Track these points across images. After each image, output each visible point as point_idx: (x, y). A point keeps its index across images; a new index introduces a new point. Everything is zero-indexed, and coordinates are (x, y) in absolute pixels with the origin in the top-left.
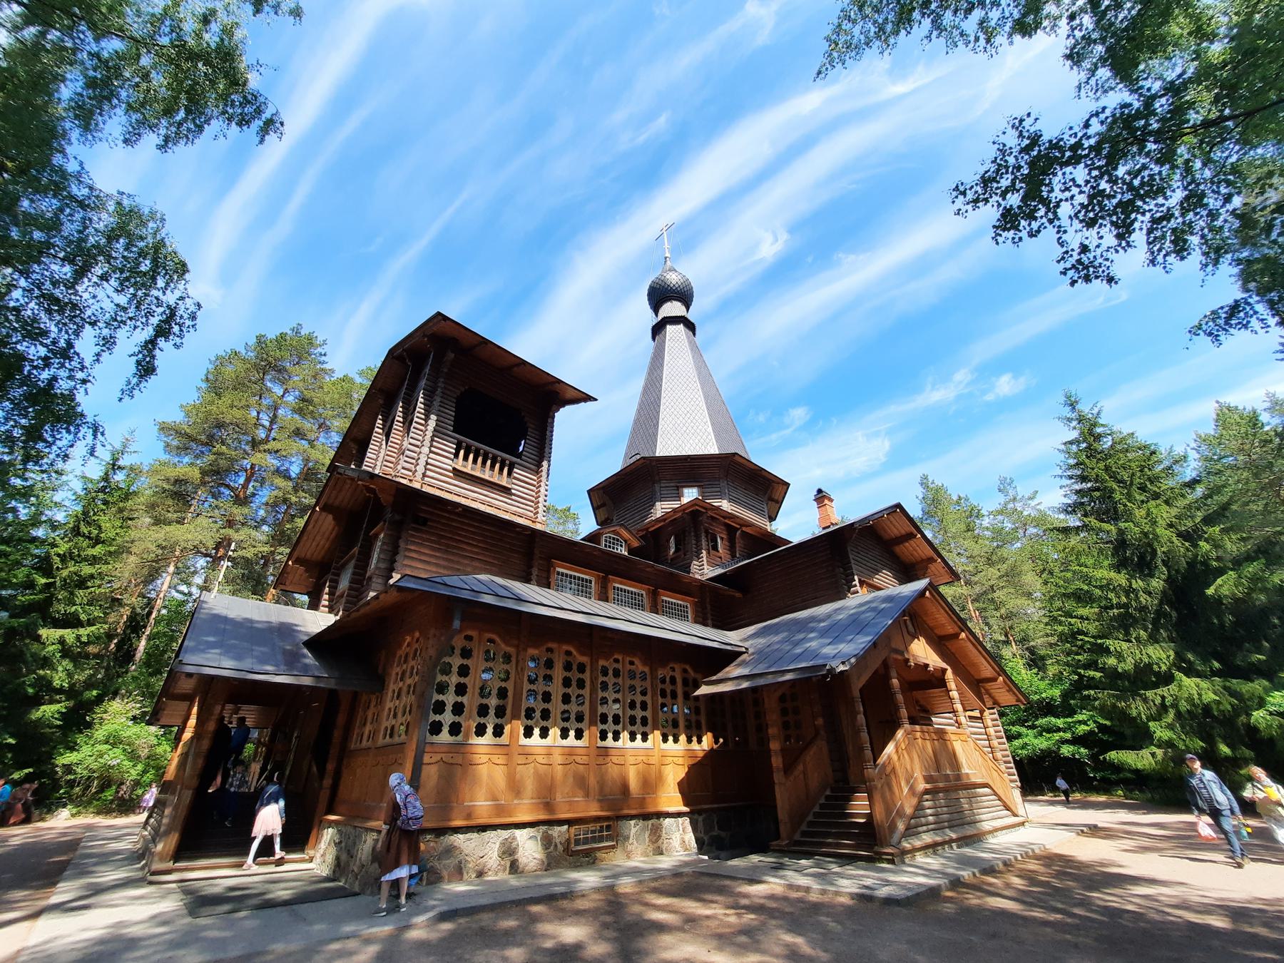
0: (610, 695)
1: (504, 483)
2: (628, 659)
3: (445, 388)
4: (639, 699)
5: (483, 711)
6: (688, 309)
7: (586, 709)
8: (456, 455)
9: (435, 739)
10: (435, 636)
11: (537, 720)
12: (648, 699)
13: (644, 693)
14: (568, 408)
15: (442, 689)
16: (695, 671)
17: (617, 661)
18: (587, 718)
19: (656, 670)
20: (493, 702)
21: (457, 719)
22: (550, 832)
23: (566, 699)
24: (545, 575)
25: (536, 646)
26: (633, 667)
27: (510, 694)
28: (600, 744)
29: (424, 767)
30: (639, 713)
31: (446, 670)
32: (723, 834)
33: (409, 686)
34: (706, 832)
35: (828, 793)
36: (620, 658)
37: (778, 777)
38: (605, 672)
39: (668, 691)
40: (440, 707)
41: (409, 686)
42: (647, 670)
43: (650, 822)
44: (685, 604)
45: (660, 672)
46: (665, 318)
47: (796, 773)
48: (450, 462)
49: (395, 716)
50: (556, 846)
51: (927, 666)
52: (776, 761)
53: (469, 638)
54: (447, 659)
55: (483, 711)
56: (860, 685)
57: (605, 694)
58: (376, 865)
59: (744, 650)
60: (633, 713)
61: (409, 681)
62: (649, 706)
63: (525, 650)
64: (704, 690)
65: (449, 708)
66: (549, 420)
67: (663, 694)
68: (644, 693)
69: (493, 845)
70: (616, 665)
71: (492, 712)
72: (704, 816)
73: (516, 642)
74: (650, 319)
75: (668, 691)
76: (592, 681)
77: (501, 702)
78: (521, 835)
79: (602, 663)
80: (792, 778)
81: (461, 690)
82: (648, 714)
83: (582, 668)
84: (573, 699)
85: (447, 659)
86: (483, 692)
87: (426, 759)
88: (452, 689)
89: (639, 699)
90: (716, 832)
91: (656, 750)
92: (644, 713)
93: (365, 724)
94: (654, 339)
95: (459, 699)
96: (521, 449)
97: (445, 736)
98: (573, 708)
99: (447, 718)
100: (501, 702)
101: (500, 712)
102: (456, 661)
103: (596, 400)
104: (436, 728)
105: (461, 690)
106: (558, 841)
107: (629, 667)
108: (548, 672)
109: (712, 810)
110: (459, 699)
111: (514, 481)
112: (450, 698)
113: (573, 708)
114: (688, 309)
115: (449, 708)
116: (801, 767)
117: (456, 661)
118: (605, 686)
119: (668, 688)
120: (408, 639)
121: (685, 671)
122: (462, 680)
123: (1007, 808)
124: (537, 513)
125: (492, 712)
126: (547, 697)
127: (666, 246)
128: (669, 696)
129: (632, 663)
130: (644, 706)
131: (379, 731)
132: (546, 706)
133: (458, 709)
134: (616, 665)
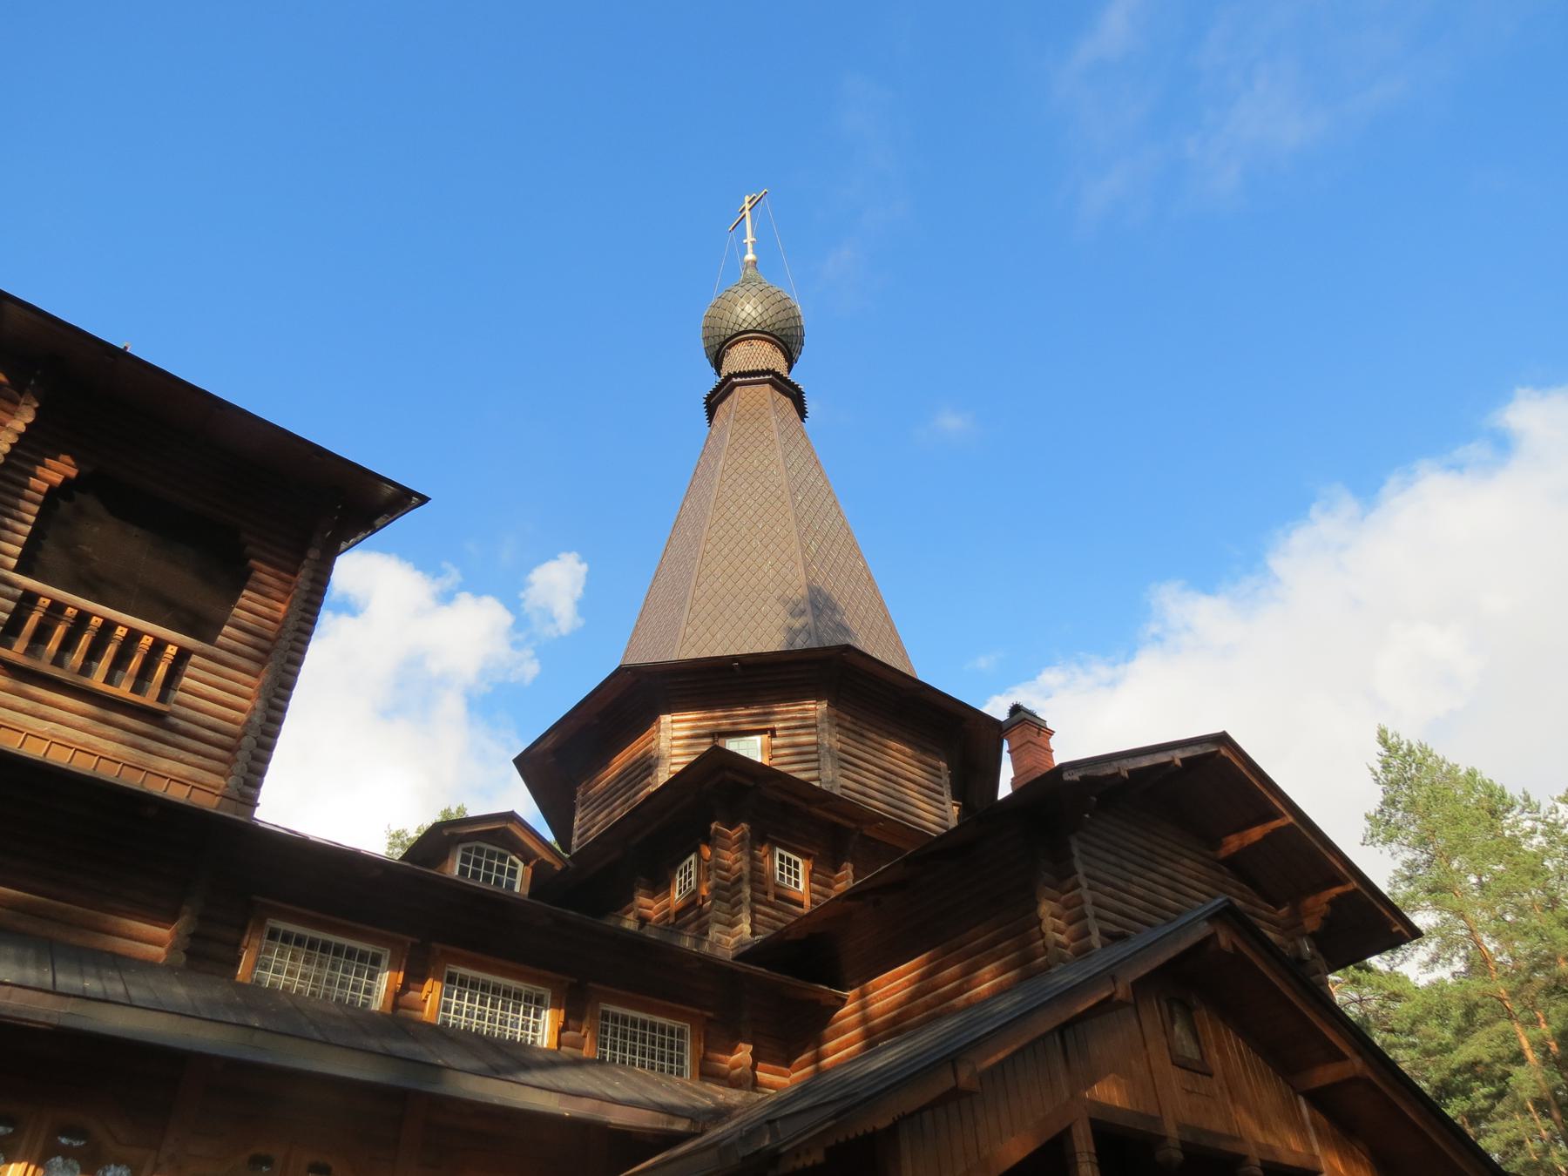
6: (790, 361)
44: (676, 1024)
46: (730, 376)
114: (790, 361)
127: (749, 239)
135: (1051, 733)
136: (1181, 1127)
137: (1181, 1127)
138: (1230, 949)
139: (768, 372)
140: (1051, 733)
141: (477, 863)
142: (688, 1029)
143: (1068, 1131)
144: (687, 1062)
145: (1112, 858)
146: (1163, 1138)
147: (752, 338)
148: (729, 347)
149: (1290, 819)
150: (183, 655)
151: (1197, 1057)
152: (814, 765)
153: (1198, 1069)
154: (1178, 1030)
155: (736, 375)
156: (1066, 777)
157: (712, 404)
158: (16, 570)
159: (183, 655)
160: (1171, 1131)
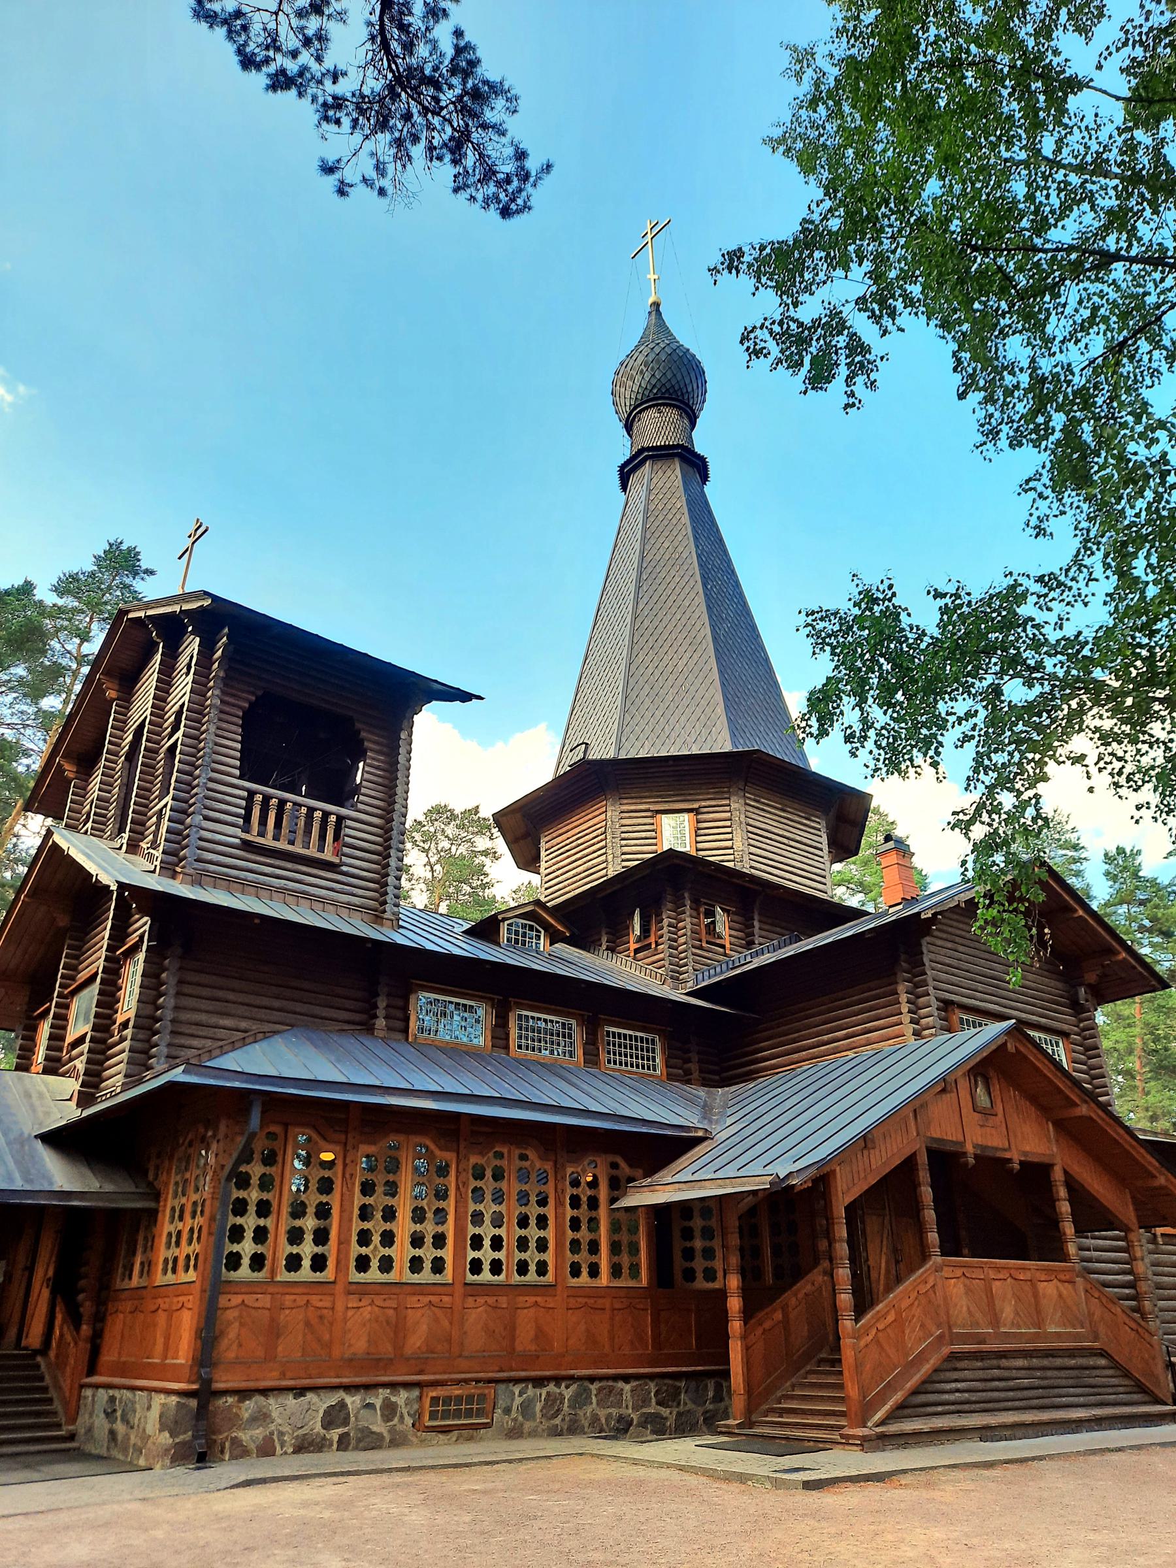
0: (489, 1208)
1: (328, 855)
2: (517, 1152)
3: (222, 712)
4: (534, 1211)
5: (296, 1236)
7: (449, 1228)
8: (247, 818)
9: (234, 1275)
10: (226, 1136)
11: (376, 1247)
12: (549, 1211)
13: (543, 1202)
14: (435, 704)
15: (240, 1208)
16: (631, 1166)
17: (499, 1155)
18: (450, 1241)
19: (564, 1167)
20: (309, 1223)
21: (260, 1249)
22: (393, 1399)
23: (418, 1215)
24: (400, 1003)
25: (374, 1143)
26: (526, 1164)
27: (335, 1212)
28: (471, 1278)
29: (219, 1312)
30: (533, 1233)
31: (243, 1182)
32: (665, 1412)
33: (195, 1204)
34: (635, 1409)
35: (823, 1355)
36: (505, 1151)
37: (736, 1326)
38: (479, 1176)
39: (584, 1199)
40: (237, 1234)
41: (195, 1204)
42: (548, 1166)
43: (544, 1392)
44: (650, 1036)
45: (569, 1170)
47: (767, 1325)
48: (238, 832)
49: (178, 1244)
50: (402, 1417)
51: (1010, 1161)
52: (734, 1304)
53: (272, 1136)
54: (243, 1168)
55: (296, 1236)
56: (848, 1199)
57: (481, 1207)
58: (167, 1434)
59: (700, 1134)
60: (523, 1232)
61: (194, 1197)
62: (551, 1222)
63: (355, 1147)
64: (631, 1200)
65: (249, 1234)
66: (403, 735)
67: (575, 1202)
68: (543, 1202)
69: (314, 1414)
70: (498, 1162)
71: (309, 1237)
72: (634, 1383)
73: (343, 1137)
74: (622, 449)
75: (584, 1199)
76: (458, 1188)
77: (321, 1223)
78: (353, 1402)
79: (474, 1160)
80: (759, 1331)
81: (264, 1209)
82: (550, 1234)
83: (443, 1171)
84: (430, 1215)
85: (243, 1169)
86: (298, 1211)
87: (223, 1301)
88: (252, 1209)
89: (534, 1211)
90: (653, 1408)
91: (559, 1288)
92: (542, 1234)
93: (134, 1254)
94: (624, 487)
95: (262, 1222)
96: (358, 780)
97: (244, 1272)
98: (429, 1228)
99: (247, 1247)
100: (321, 1223)
101: (321, 1237)
102: (256, 1170)
103: (480, 698)
104: (234, 1261)
105: (264, 1209)
106: (405, 1411)
107: (519, 1163)
108: (391, 1177)
109: (651, 1377)
110: (262, 1222)
111: (346, 850)
112: (250, 1222)
113: (429, 1228)
115: (249, 1234)
116: (778, 1316)
117: (256, 1170)
118: (478, 1195)
119: (584, 1193)
120: (190, 1136)
121: (614, 1166)
122: (265, 1196)
123: (1141, 1388)
124: (385, 903)
125: (309, 1237)
126: (389, 1214)
128: (585, 1206)
129: (524, 1157)
130: (542, 1222)
131: (156, 1264)
132: (388, 1226)
133: (261, 1235)
134: (498, 1162)
135: (913, 854)
136: (975, 1146)
137: (975, 1146)
138: (1014, 1051)
139: (678, 446)
140: (913, 854)
141: (517, 933)
142: (657, 1039)
143: (914, 1154)
144: (657, 1060)
145: (949, 945)
146: (964, 1154)
147: (661, 405)
148: (640, 412)
149: (1081, 913)
150: (340, 819)
151: (989, 1105)
152: (729, 836)
153: (987, 1113)
154: (980, 1091)
155: (649, 449)
156: (923, 916)
157: (626, 474)
158: (240, 778)
159: (340, 819)
160: (969, 1148)
